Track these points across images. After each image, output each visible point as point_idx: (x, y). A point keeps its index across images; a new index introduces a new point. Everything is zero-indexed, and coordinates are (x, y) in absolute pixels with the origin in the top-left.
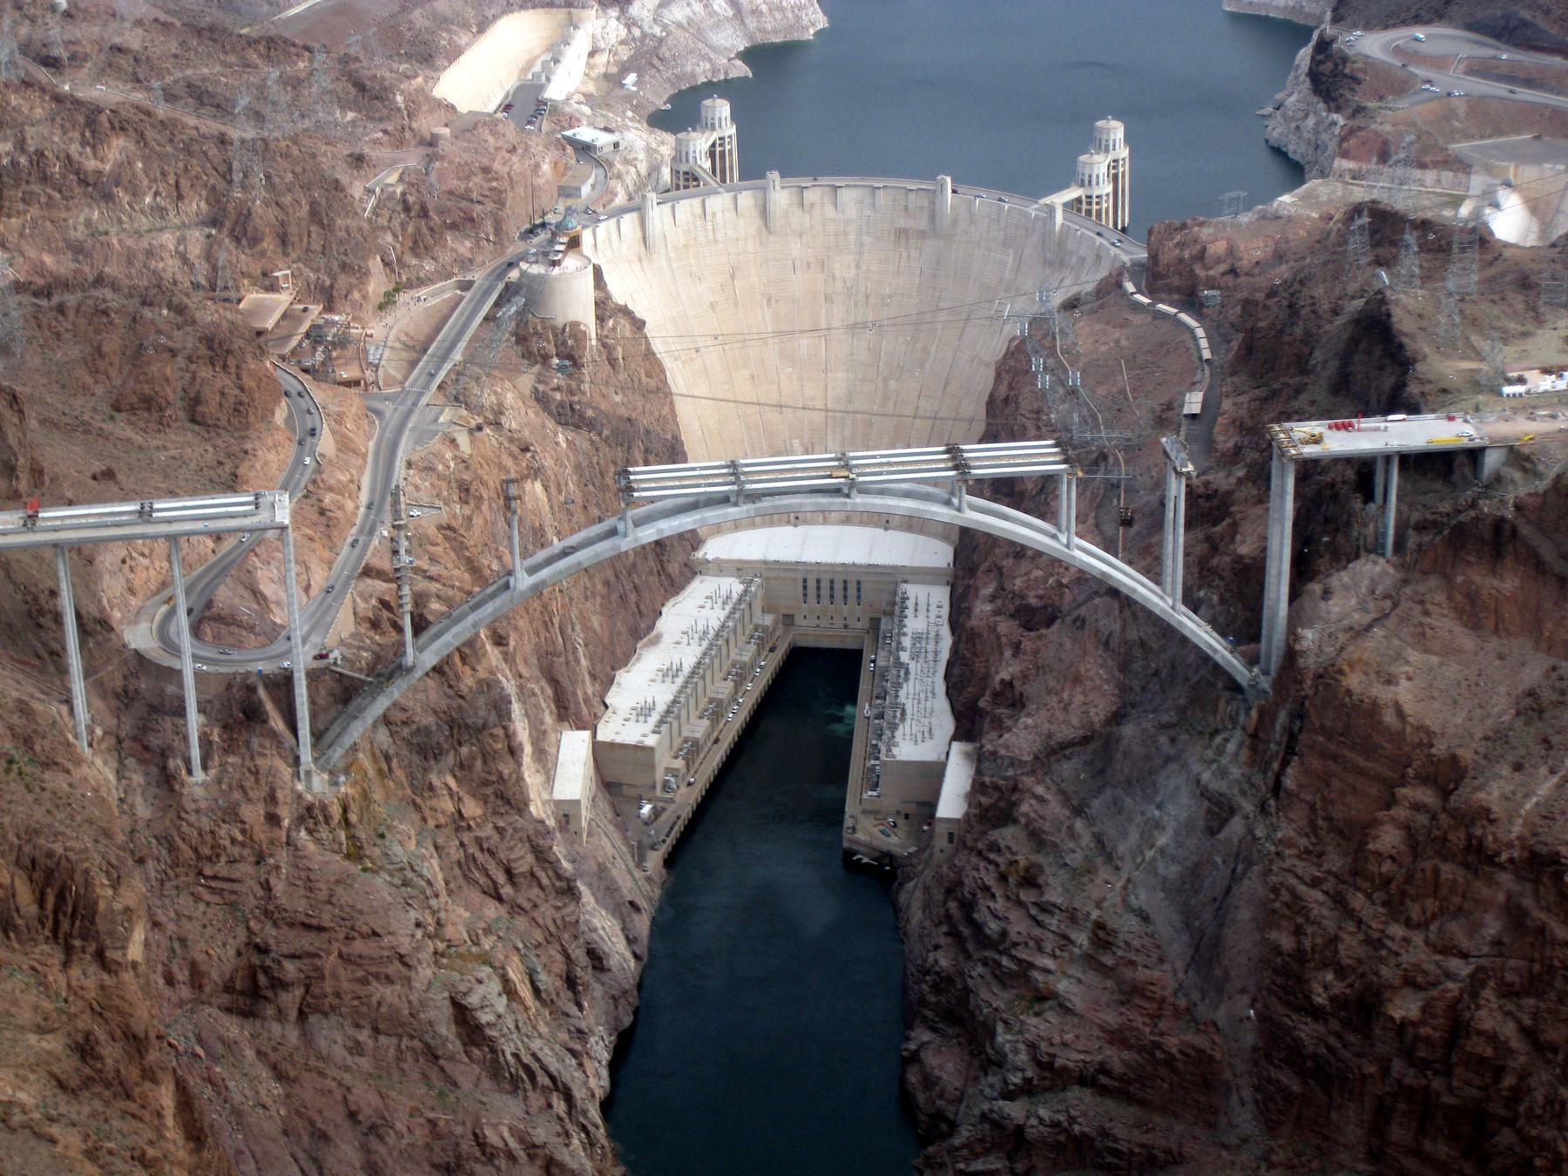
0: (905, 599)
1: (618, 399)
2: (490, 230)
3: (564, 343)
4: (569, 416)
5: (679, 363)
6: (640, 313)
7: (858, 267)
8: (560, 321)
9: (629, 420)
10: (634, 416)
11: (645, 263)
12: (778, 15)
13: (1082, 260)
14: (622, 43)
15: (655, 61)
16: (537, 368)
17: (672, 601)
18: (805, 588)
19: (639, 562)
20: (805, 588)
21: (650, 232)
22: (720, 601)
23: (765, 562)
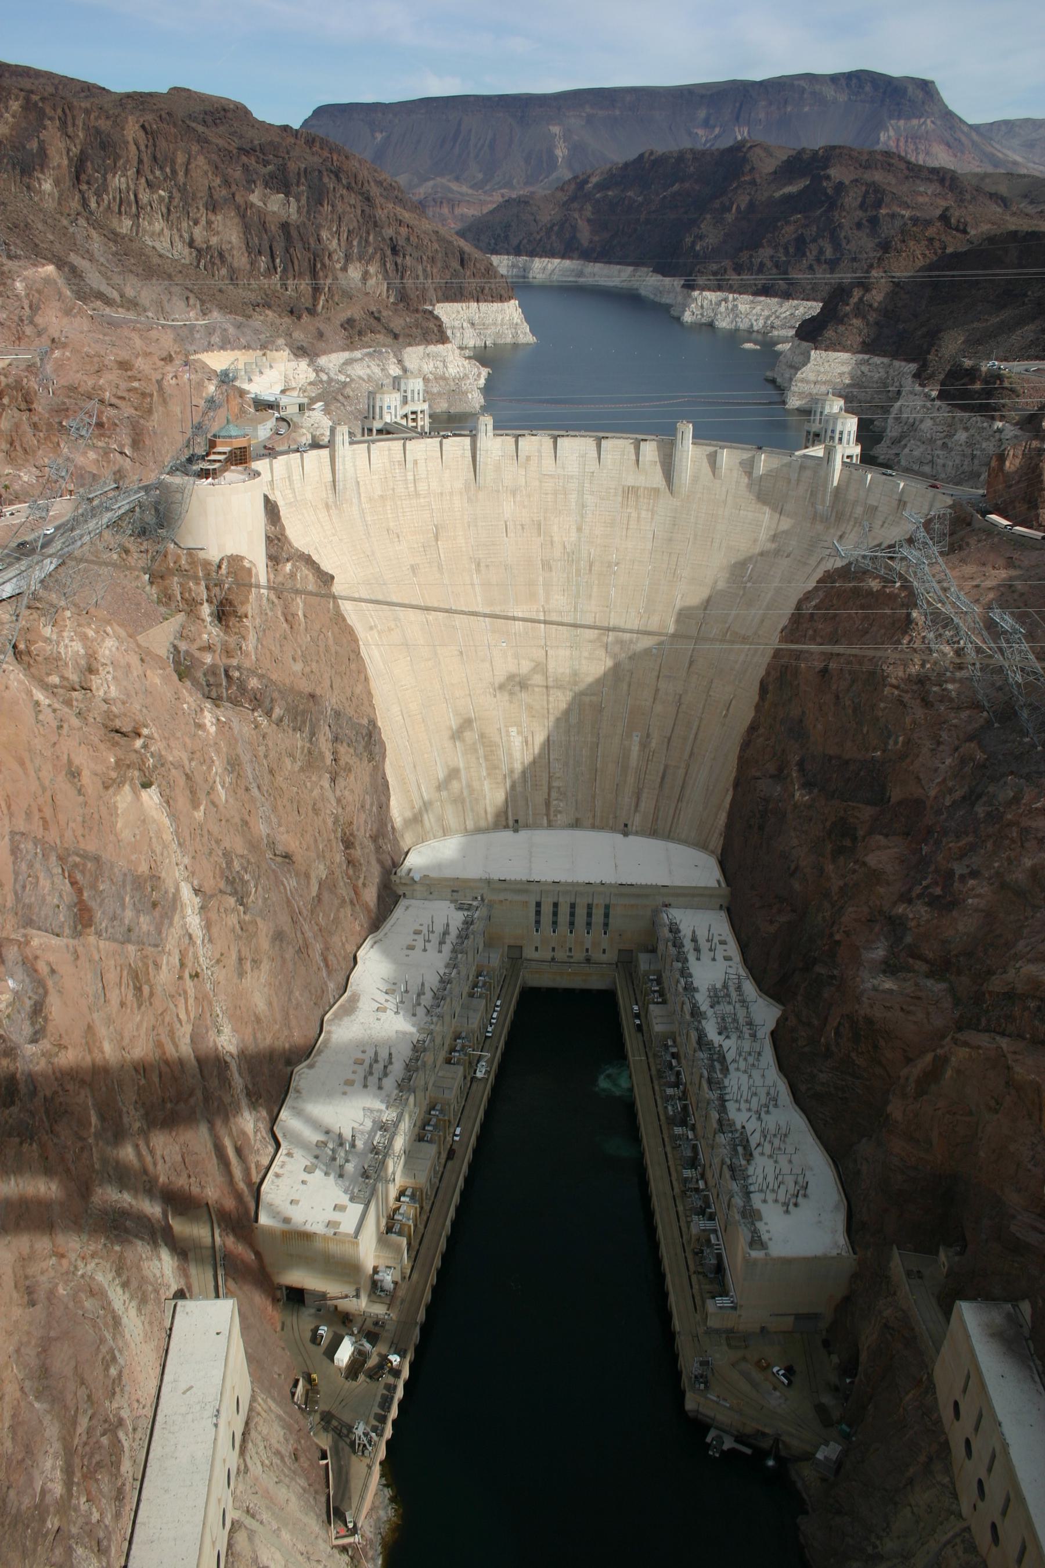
0: (674, 929)
1: (298, 667)
2: (127, 441)
3: (219, 584)
4: (223, 686)
5: (375, 632)
6: (326, 566)
7: (579, 529)
8: (214, 555)
9: (312, 696)
10: (318, 692)
11: (333, 511)
12: (442, 383)
13: (872, 510)
14: (311, 383)
15: (340, 398)
16: (181, 617)
18: (538, 913)
19: (326, 896)
20: (538, 913)
21: (339, 476)
22: (435, 938)
23: (489, 882)
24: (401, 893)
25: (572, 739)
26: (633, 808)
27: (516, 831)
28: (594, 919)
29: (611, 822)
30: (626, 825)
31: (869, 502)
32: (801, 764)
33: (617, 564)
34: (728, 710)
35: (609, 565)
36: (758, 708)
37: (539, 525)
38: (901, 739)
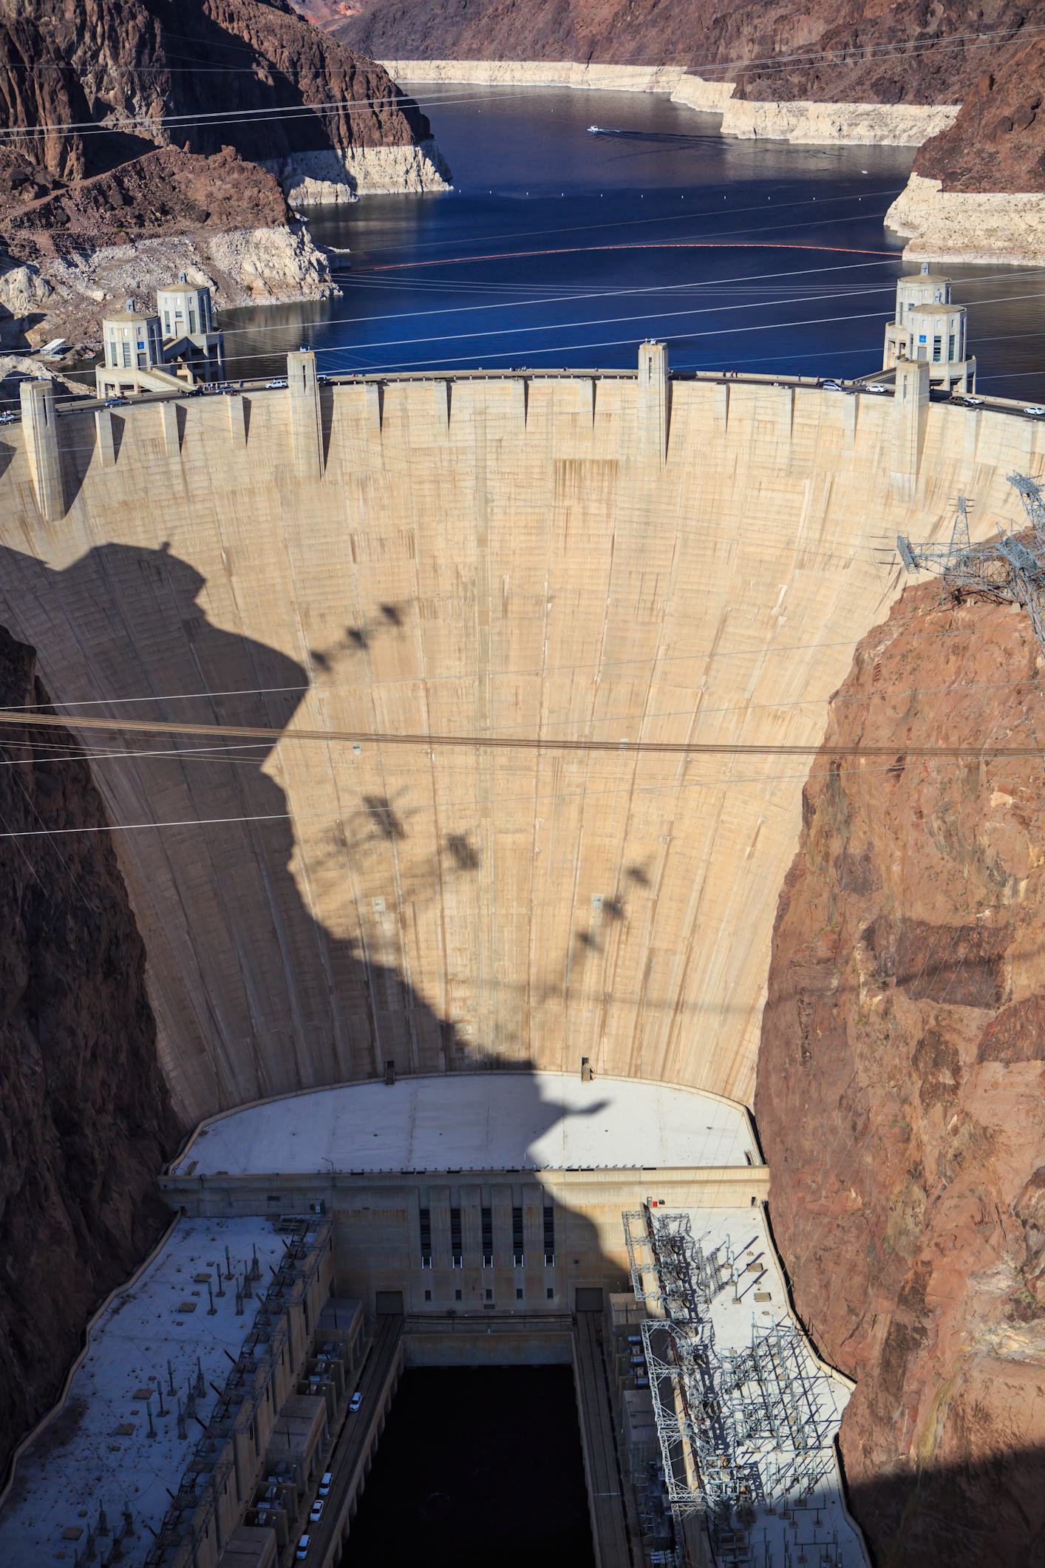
7: (482, 542)
17: (112, 1300)
18: (425, 1229)
20: (425, 1229)
22: (231, 1288)
24: (177, 1207)
25: (484, 912)
26: (597, 1029)
27: (390, 1082)
28: (526, 1235)
29: (558, 1056)
30: (585, 1061)
31: (980, 460)
32: (869, 936)
33: (550, 599)
34: (753, 845)
35: (538, 602)
36: (804, 838)
37: (411, 538)
38: (1023, 885)
